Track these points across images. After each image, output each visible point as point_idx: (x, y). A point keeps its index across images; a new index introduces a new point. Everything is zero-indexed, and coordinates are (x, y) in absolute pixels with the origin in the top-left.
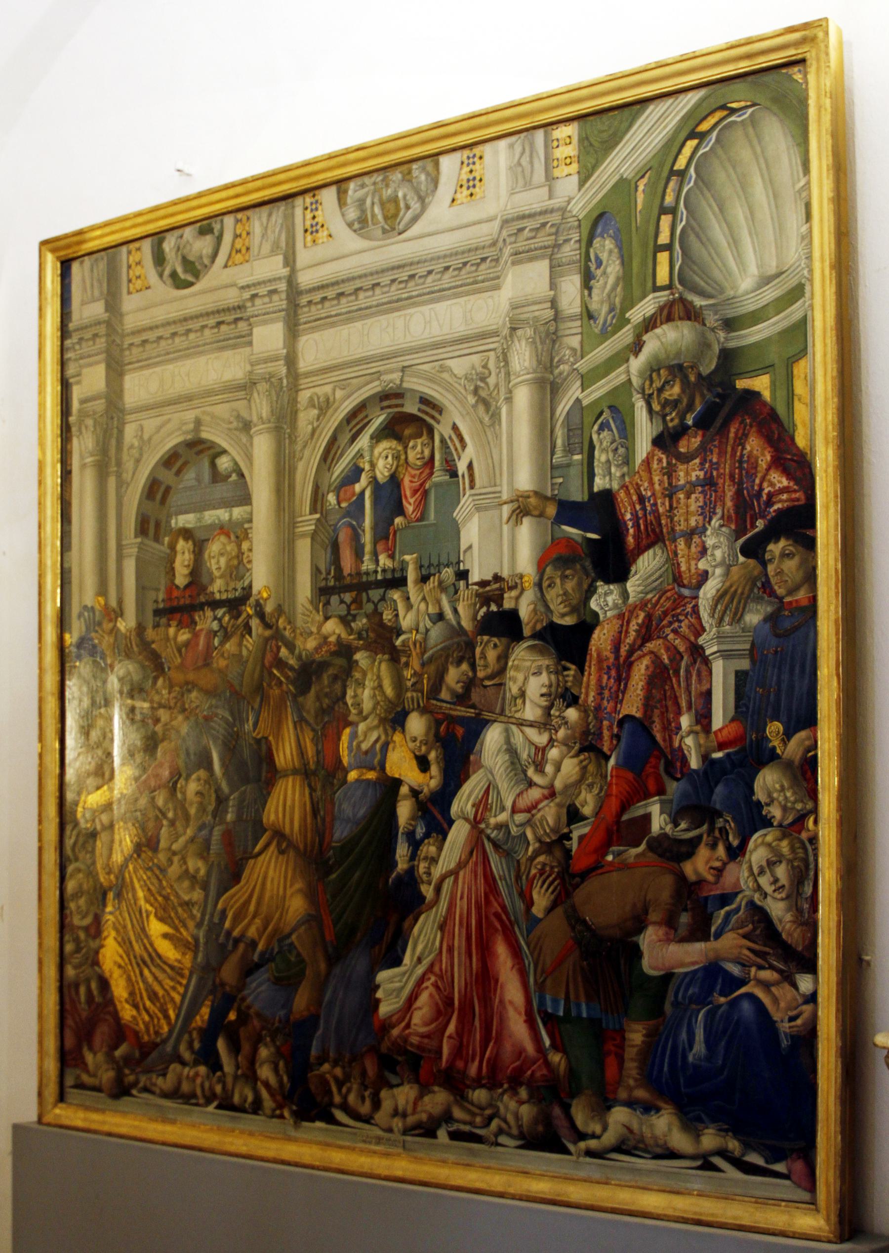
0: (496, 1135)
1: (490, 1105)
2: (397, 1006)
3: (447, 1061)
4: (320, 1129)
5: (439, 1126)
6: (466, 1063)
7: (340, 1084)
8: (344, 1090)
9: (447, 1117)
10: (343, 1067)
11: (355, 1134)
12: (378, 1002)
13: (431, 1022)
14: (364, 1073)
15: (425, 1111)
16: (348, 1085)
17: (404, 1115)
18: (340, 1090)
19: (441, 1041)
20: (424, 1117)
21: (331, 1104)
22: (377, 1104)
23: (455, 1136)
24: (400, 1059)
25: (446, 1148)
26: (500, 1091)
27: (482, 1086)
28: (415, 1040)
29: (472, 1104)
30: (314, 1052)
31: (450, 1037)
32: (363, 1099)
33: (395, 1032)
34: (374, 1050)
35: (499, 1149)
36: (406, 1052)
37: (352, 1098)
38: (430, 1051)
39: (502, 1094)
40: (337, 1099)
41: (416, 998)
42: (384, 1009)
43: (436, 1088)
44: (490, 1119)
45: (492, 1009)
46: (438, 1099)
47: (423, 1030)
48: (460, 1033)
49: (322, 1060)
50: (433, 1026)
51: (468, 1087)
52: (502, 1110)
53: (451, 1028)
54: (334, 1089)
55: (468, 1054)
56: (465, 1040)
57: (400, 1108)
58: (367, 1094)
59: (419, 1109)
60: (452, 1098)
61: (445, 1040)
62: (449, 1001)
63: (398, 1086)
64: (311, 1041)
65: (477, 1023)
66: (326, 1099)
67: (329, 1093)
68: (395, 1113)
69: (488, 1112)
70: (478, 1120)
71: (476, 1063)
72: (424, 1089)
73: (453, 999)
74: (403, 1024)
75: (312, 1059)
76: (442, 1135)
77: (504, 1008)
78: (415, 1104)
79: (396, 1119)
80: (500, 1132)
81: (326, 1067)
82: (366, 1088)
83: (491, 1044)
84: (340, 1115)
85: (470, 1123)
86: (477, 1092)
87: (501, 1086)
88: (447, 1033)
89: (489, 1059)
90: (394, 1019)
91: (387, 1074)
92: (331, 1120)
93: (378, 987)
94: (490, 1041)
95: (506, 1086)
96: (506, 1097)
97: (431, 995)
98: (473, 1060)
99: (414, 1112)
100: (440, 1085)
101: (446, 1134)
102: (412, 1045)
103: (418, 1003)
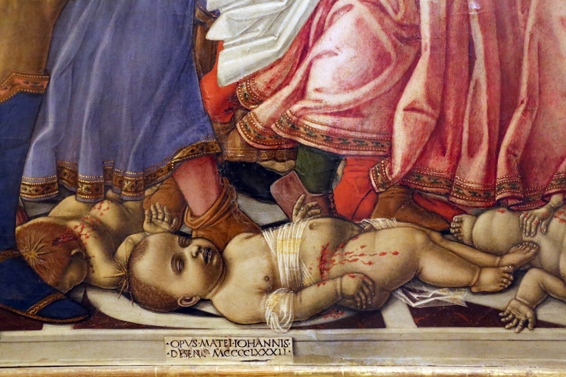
0: (534, 306)
1: (519, 244)
2: (268, 52)
3: (406, 161)
4: (55, 341)
5: (390, 299)
6: (456, 159)
7: (110, 239)
8: (123, 250)
9: (411, 279)
10: (119, 202)
11: (155, 340)
12: (214, 48)
13: (376, 74)
14: (180, 207)
15: (352, 274)
16: (136, 237)
17: (296, 287)
18: (111, 254)
19: (391, 118)
20: (349, 285)
21: (89, 283)
22: (218, 270)
23: (426, 317)
24: (279, 167)
25: (406, 344)
26: (543, 210)
27: (497, 205)
28: (320, 122)
29: (472, 245)
30: (30, 176)
31: (411, 108)
32: (179, 263)
33: (264, 111)
34: (206, 155)
35: (542, 332)
36: (295, 149)
37: (146, 268)
38: (360, 143)
39: (548, 218)
40: (104, 271)
41: (320, 32)
42: (230, 66)
43: (379, 222)
44: (518, 273)
45: (518, 38)
46: (385, 244)
47: (345, 98)
48: (437, 100)
49: (53, 192)
50: (365, 89)
51: (461, 211)
52: (547, 251)
53: (415, 90)
54: (95, 250)
55: (458, 138)
56: (450, 114)
57: (284, 275)
58: (188, 252)
59: (335, 269)
60: (419, 238)
61: (399, 116)
62: (407, 33)
63: (276, 225)
64: (24, 155)
65: (480, 72)
66: (72, 275)
67: (85, 259)
68: (272, 284)
69: (512, 259)
70: (488, 277)
71: (481, 158)
72: (346, 224)
73: (417, 28)
74: (286, 91)
75: (25, 194)
76: (398, 317)
77: (550, 34)
78: (324, 261)
79: (272, 298)
80: (545, 295)
81: (69, 204)
82: (186, 239)
83: (518, 115)
84: (110, 304)
85: (468, 287)
86: (483, 219)
87: (545, 199)
88: (404, 101)
89: (513, 146)
90: (261, 83)
91: (245, 203)
92: (88, 316)
93: (214, 15)
94: (515, 107)
95: (555, 200)
96: (555, 223)
97: (359, 22)
98: (472, 154)
99: (322, 276)
100: (388, 215)
101: (408, 315)
102: (311, 134)
103: (326, 43)
